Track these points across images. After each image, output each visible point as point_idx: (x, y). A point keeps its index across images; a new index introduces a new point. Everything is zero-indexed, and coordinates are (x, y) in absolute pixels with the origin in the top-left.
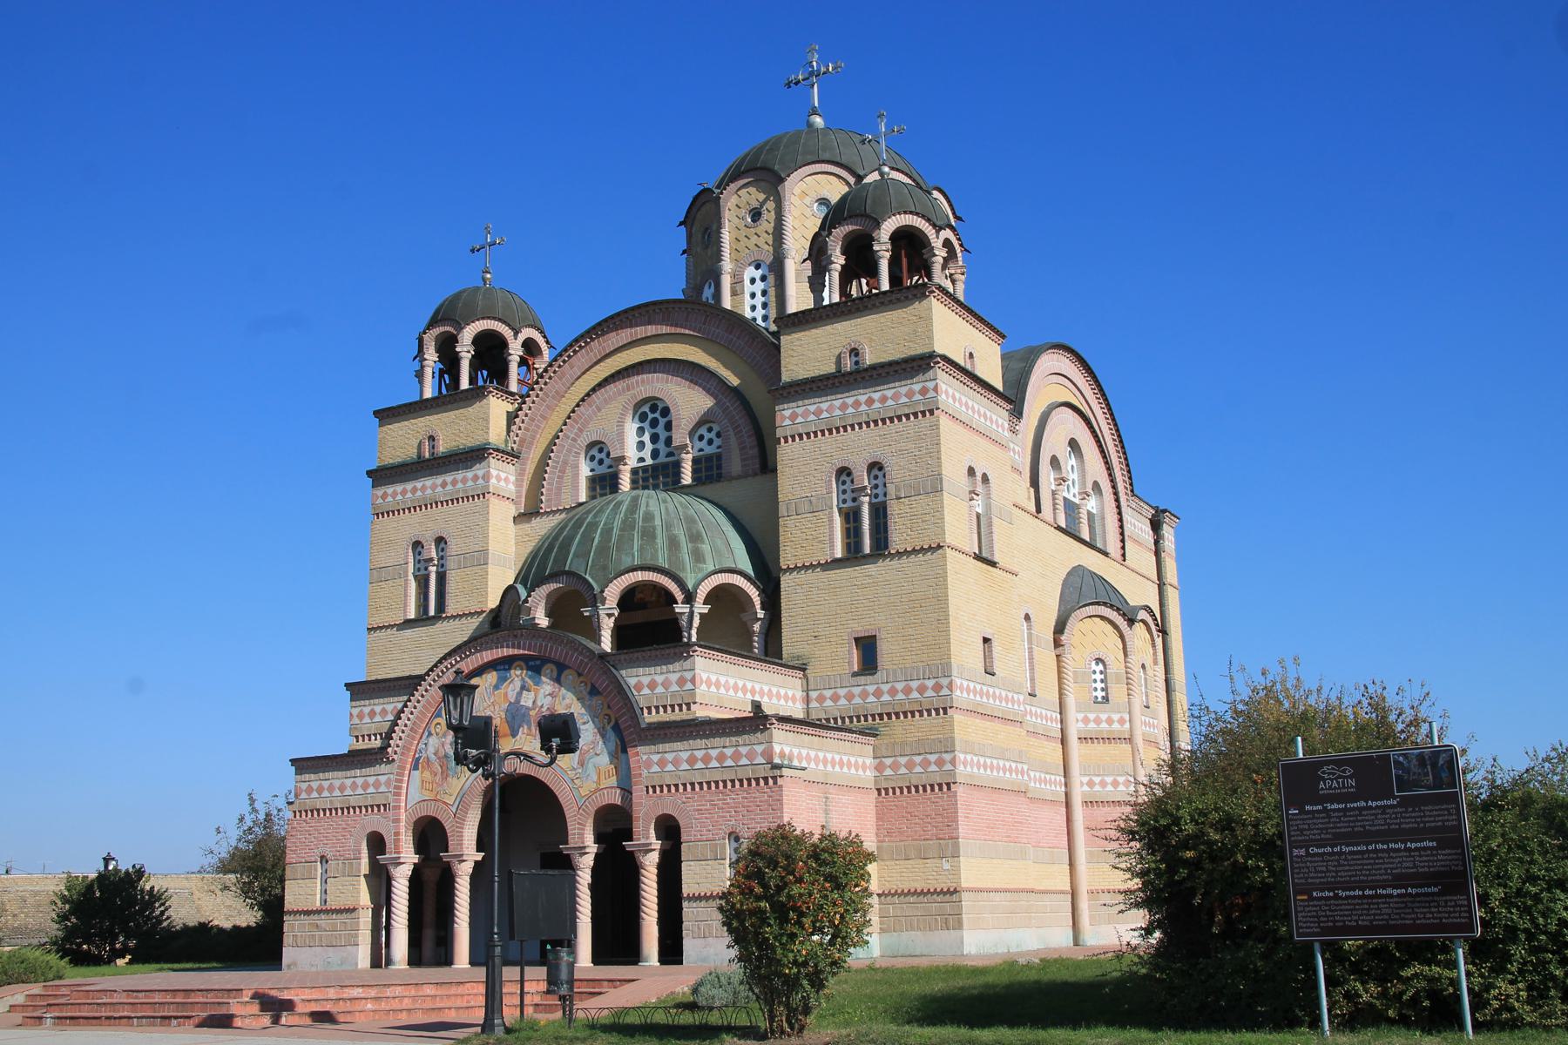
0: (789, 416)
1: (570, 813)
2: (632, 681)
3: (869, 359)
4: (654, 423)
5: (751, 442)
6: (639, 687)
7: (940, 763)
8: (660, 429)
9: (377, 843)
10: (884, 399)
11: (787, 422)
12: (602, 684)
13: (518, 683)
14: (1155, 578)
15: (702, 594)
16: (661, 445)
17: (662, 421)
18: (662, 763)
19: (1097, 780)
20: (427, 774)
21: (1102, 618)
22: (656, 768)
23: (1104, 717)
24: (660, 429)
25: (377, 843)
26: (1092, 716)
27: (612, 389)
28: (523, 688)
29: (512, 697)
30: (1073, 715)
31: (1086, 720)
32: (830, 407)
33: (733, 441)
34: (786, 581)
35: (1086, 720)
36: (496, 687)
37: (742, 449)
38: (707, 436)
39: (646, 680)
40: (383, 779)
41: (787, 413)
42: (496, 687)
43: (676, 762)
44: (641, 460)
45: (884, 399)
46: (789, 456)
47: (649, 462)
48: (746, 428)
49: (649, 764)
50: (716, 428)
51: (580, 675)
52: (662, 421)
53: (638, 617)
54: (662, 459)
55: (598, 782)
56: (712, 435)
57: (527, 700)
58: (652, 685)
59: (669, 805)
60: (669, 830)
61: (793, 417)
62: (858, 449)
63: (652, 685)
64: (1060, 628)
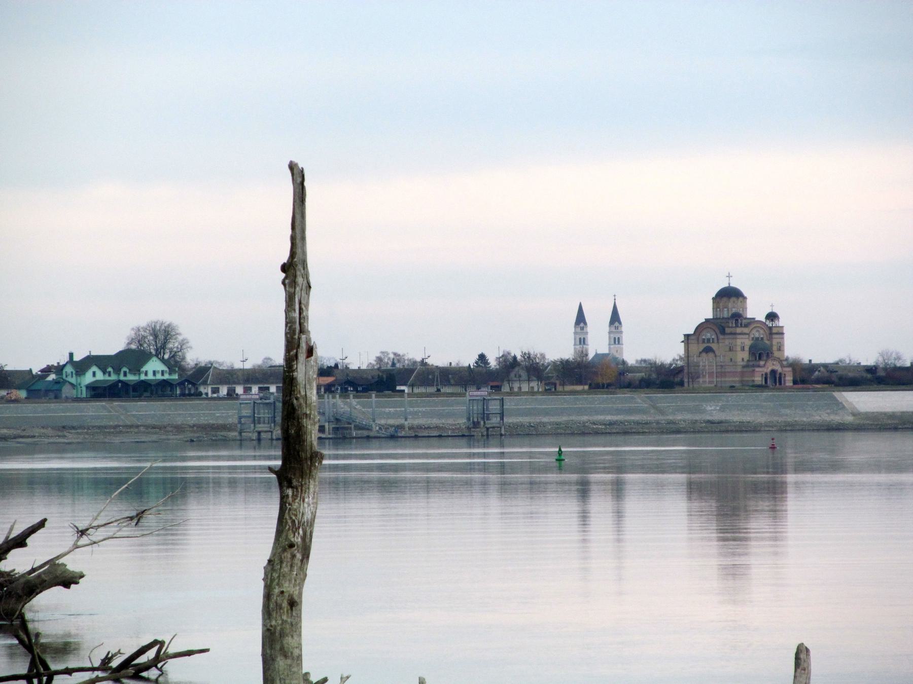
0: (774, 336)
9: (762, 375)
60: (785, 374)
62: (779, 340)
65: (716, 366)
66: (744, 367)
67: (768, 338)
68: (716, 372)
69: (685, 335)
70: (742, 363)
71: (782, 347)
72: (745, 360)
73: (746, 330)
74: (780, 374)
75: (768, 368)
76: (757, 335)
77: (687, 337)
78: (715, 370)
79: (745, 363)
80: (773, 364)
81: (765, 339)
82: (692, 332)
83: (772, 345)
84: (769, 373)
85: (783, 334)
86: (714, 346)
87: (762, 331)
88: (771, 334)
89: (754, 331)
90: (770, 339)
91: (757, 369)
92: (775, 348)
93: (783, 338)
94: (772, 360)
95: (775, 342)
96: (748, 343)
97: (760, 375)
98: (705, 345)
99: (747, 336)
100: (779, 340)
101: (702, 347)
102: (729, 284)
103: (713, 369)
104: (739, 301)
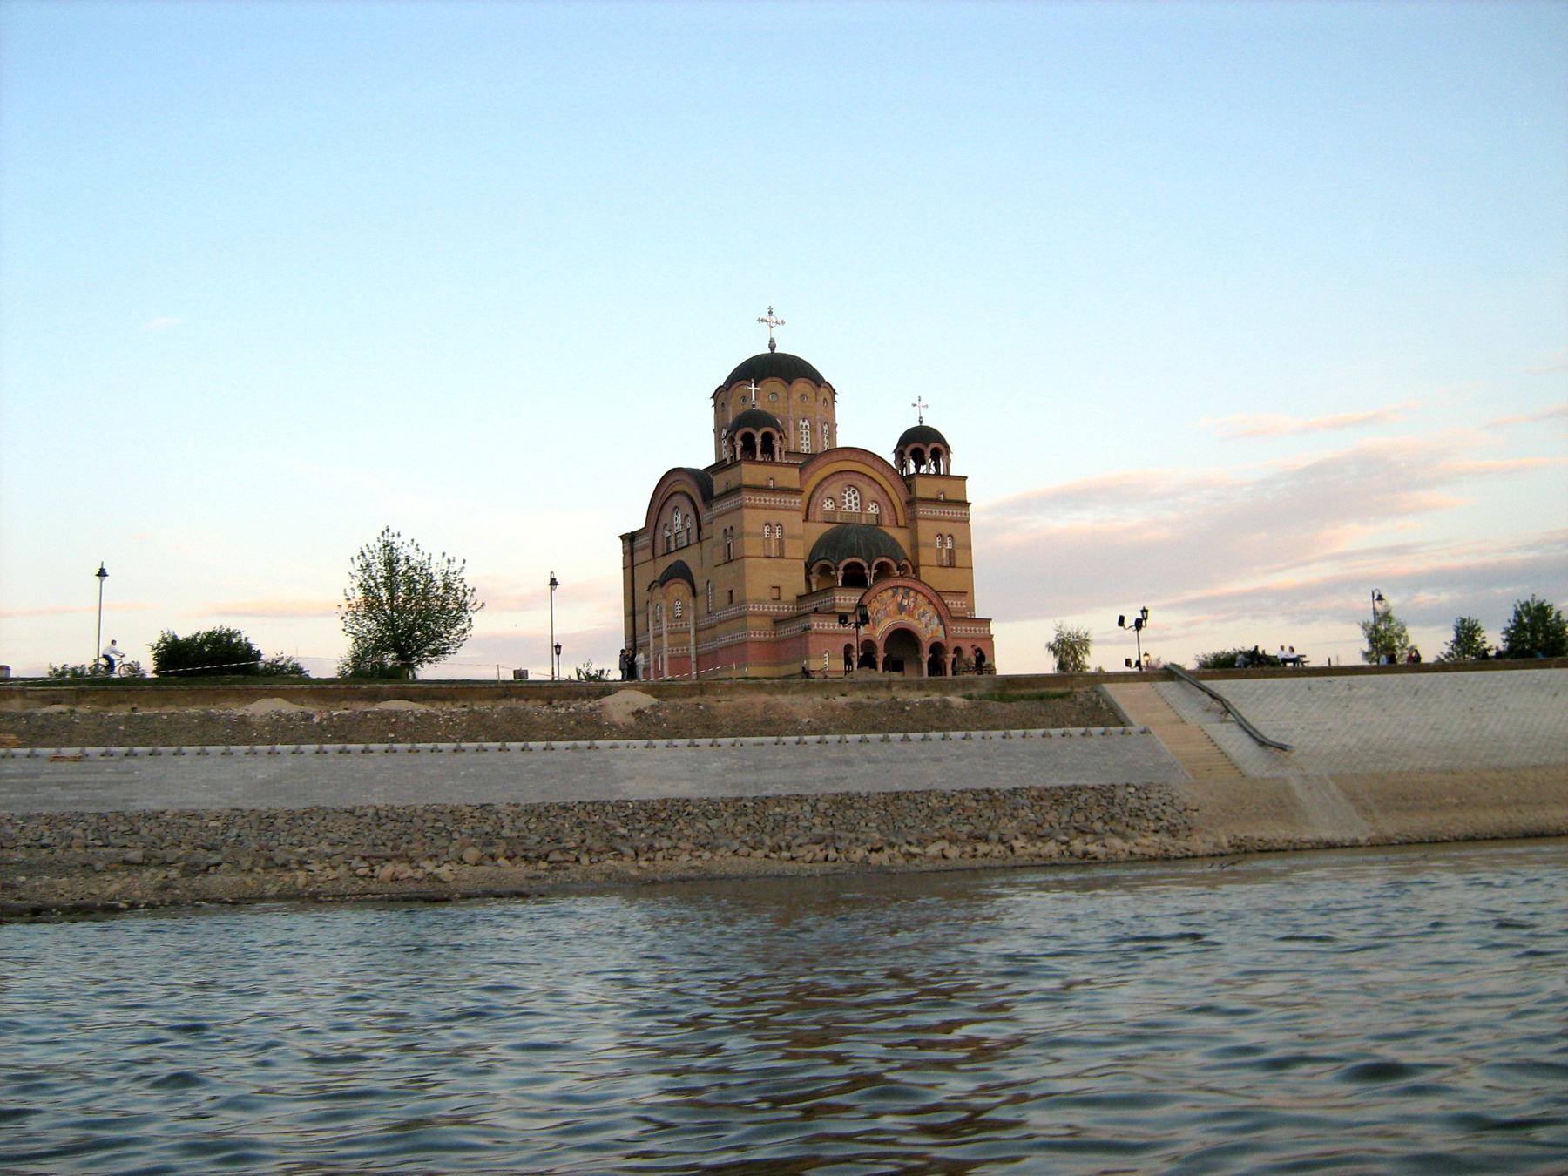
1: (924, 644)
3: (948, 497)
4: (849, 495)
9: (848, 648)
12: (935, 601)
16: (853, 505)
27: (836, 478)
29: (899, 600)
32: (936, 511)
36: (893, 596)
42: (893, 596)
46: (922, 524)
48: (890, 508)
51: (924, 595)
53: (850, 572)
57: (905, 602)
62: (946, 528)
65: (697, 631)
66: (778, 622)
67: (902, 523)
68: (698, 657)
69: (621, 537)
70: (772, 608)
71: (959, 555)
72: (789, 594)
73: (789, 477)
74: (937, 648)
76: (851, 503)
77: (629, 539)
78: (693, 650)
79: (783, 609)
80: (901, 608)
81: (886, 520)
82: (637, 522)
83: (915, 546)
84: (880, 645)
85: (966, 504)
86: (690, 557)
87: (870, 492)
88: (911, 502)
89: (834, 488)
90: (911, 522)
91: (818, 624)
92: (927, 557)
93: (967, 521)
95: (926, 530)
96: (803, 535)
97: (841, 648)
98: (671, 560)
99: (797, 501)
100: (946, 528)
101: (665, 563)
102: (772, 347)
103: (687, 643)
104: (796, 396)
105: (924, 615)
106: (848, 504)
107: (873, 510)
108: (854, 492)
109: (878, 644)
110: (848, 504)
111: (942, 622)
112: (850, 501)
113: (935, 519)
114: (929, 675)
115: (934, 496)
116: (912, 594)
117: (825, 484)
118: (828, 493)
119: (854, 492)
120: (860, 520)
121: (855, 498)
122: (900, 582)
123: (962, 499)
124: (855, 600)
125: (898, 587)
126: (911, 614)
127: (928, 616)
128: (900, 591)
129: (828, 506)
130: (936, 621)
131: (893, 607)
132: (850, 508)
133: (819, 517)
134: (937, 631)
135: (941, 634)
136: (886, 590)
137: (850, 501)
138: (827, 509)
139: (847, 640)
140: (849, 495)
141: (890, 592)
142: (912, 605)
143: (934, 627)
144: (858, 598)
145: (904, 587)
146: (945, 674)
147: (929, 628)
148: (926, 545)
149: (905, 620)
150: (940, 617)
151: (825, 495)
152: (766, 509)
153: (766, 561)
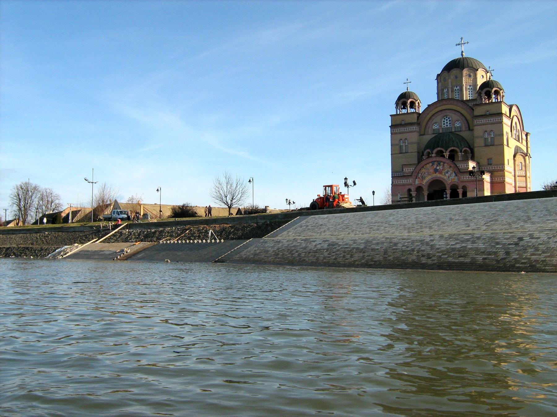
0: (477, 121)
1: (447, 185)
2: (458, 165)
4: (447, 120)
5: (467, 125)
6: (459, 166)
7: (503, 179)
8: (448, 121)
9: (409, 190)
10: (493, 120)
11: (476, 123)
13: (436, 165)
14: (526, 145)
15: (463, 150)
16: (448, 124)
17: (448, 120)
18: (464, 178)
19: (520, 183)
20: (419, 180)
21: (521, 155)
22: (462, 179)
23: (521, 172)
24: (448, 121)
25: (409, 190)
26: (519, 172)
28: (437, 166)
29: (435, 167)
30: (517, 172)
31: (519, 173)
32: (483, 121)
33: (463, 125)
34: (476, 149)
35: (519, 173)
36: (432, 166)
37: (465, 126)
38: (457, 123)
39: (460, 165)
40: (411, 180)
41: (476, 121)
43: (466, 178)
44: (444, 126)
45: (493, 120)
46: (476, 128)
47: (446, 127)
49: (461, 178)
50: (459, 122)
52: (448, 120)
54: (448, 126)
55: (452, 180)
56: (459, 123)
57: (438, 168)
58: (461, 166)
59: (464, 184)
61: (477, 122)
63: (461, 166)
64: (514, 156)
75: (423, 178)
80: (436, 171)
87: (455, 117)
92: (478, 142)
94: (433, 163)
95: (478, 130)
97: (405, 190)
100: (489, 128)
102: (462, 55)
105: (447, 173)
106: (446, 124)
107: (457, 124)
108: (449, 118)
109: (424, 187)
110: (446, 124)
111: (456, 175)
112: (447, 123)
113: (484, 124)
114: (451, 197)
115: (483, 114)
116: (442, 164)
117: (433, 117)
118: (434, 121)
119: (449, 118)
120: (452, 130)
121: (450, 121)
122: (434, 159)
123: (499, 112)
124: (413, 169)
125: (435, 161)
126: (441, 173)
127: (449, 173)
128: (436, 163)
129: (436, 127)
130: (454, 174)
131: (432, 171)
132: (447, 126)
133: (430, 132)
134: (454, 179)
135: (456, 179)
136: (428, 163)
137: (447, 123)
138: (436, 128)
139: (408, 187)
140: (447, 120)
141: (431, 164)
142: (441, 168)
143: (452, 177)
144: (414, 169)
145: (438, 161)
146: (459, 197)
147: (450, 178)
148: (478, 137)
149: (438, 175)
150: (455, 173)
151: (433, 122)
152: (400, 133)
153: (400, 155)
